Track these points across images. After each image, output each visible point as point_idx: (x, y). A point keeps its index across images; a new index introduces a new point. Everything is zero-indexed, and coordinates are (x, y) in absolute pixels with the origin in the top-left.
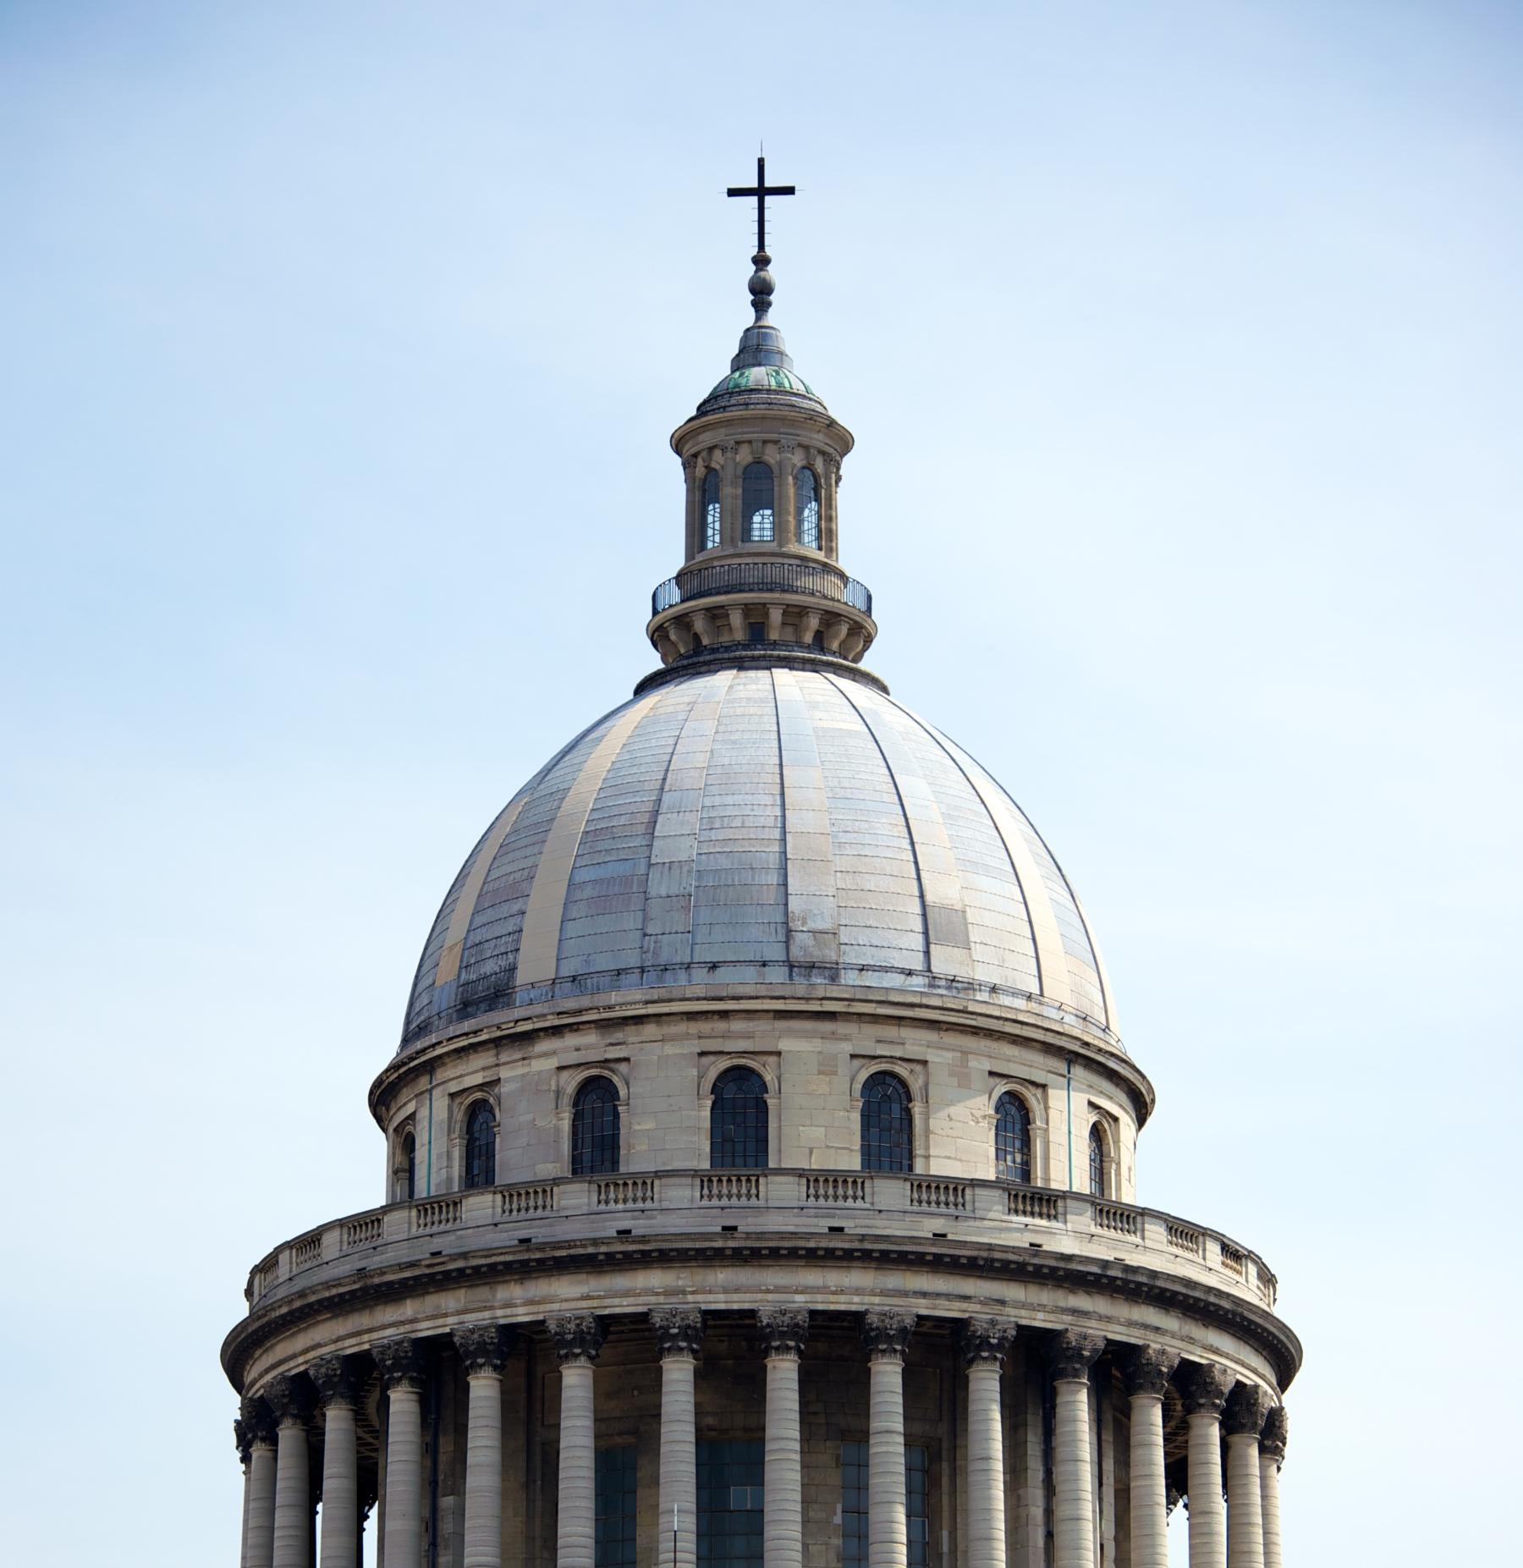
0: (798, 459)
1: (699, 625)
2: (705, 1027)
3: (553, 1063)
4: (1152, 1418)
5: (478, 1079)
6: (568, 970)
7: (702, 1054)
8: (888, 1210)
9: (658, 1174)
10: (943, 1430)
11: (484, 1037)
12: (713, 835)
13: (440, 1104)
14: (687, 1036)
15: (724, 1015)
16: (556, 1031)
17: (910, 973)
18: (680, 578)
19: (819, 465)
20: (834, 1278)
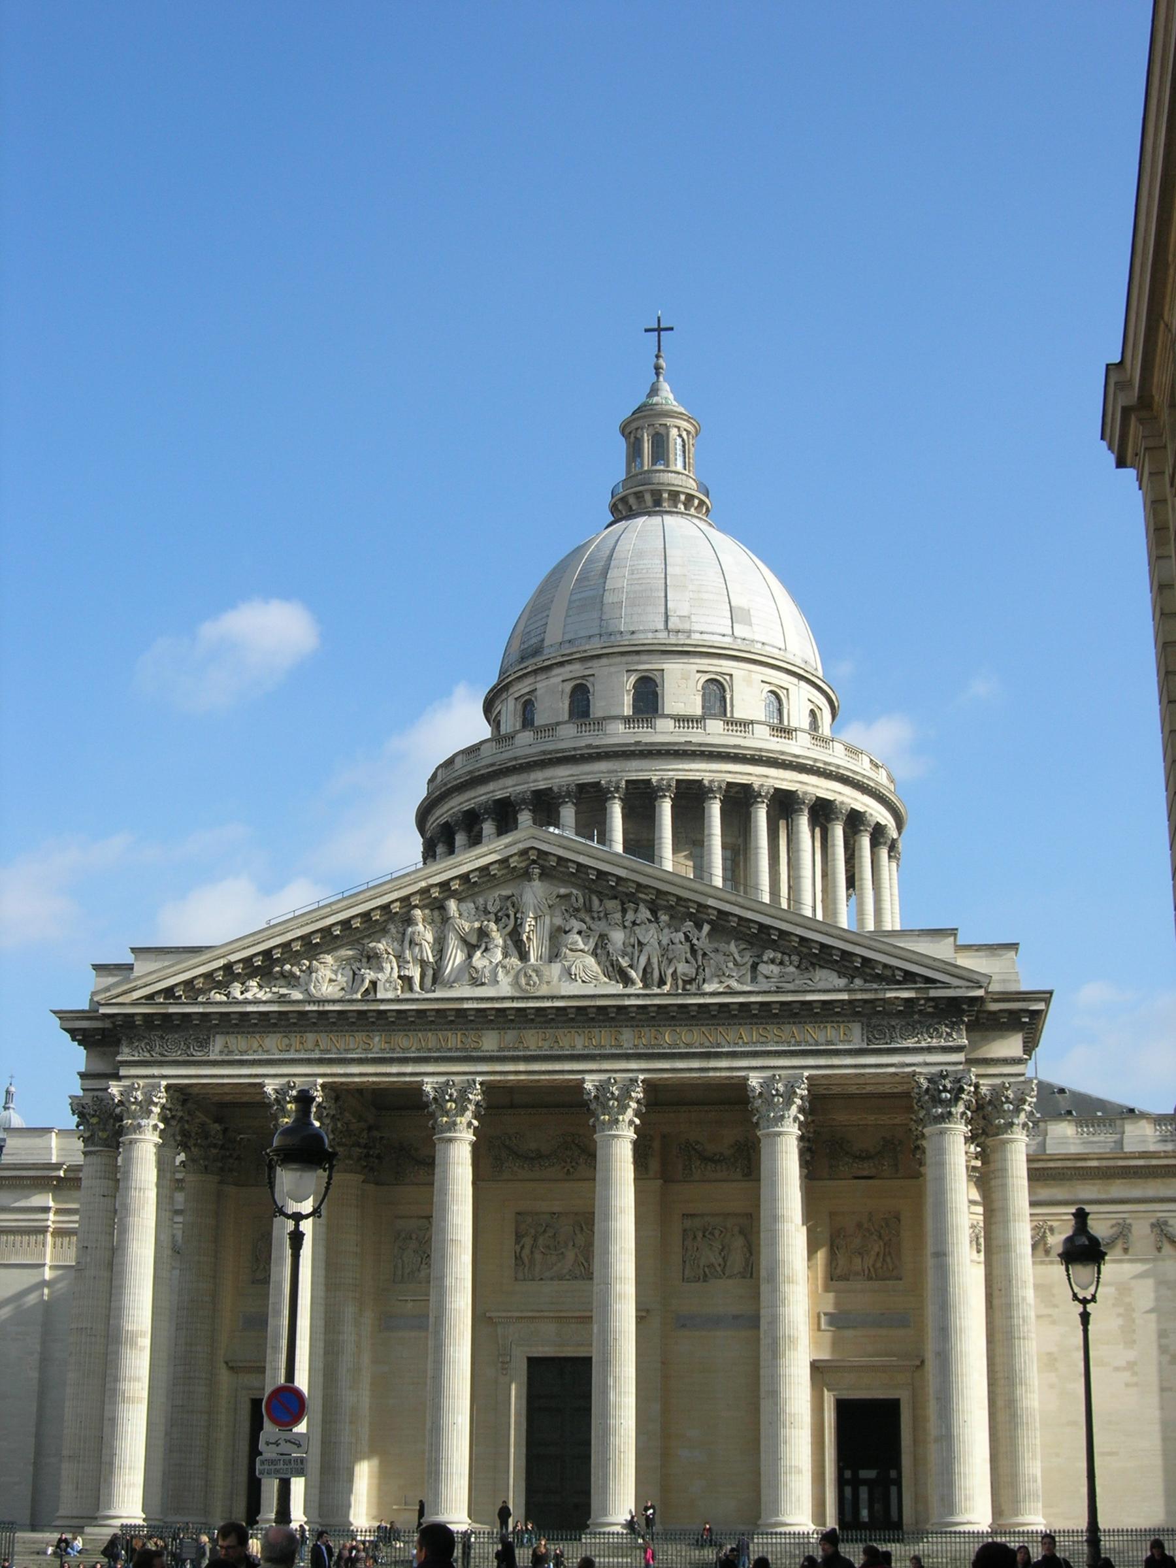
3: (561, 678)
5: (527, 690)
6: (567, 638)
8: (715, 733)
9: (604, 718)
10: (740, 841)
12: (634, 576)
13: (511, 702)
14: (621, 663)
15: (638, 653)
16: (561, 664)
19: (684, 434)
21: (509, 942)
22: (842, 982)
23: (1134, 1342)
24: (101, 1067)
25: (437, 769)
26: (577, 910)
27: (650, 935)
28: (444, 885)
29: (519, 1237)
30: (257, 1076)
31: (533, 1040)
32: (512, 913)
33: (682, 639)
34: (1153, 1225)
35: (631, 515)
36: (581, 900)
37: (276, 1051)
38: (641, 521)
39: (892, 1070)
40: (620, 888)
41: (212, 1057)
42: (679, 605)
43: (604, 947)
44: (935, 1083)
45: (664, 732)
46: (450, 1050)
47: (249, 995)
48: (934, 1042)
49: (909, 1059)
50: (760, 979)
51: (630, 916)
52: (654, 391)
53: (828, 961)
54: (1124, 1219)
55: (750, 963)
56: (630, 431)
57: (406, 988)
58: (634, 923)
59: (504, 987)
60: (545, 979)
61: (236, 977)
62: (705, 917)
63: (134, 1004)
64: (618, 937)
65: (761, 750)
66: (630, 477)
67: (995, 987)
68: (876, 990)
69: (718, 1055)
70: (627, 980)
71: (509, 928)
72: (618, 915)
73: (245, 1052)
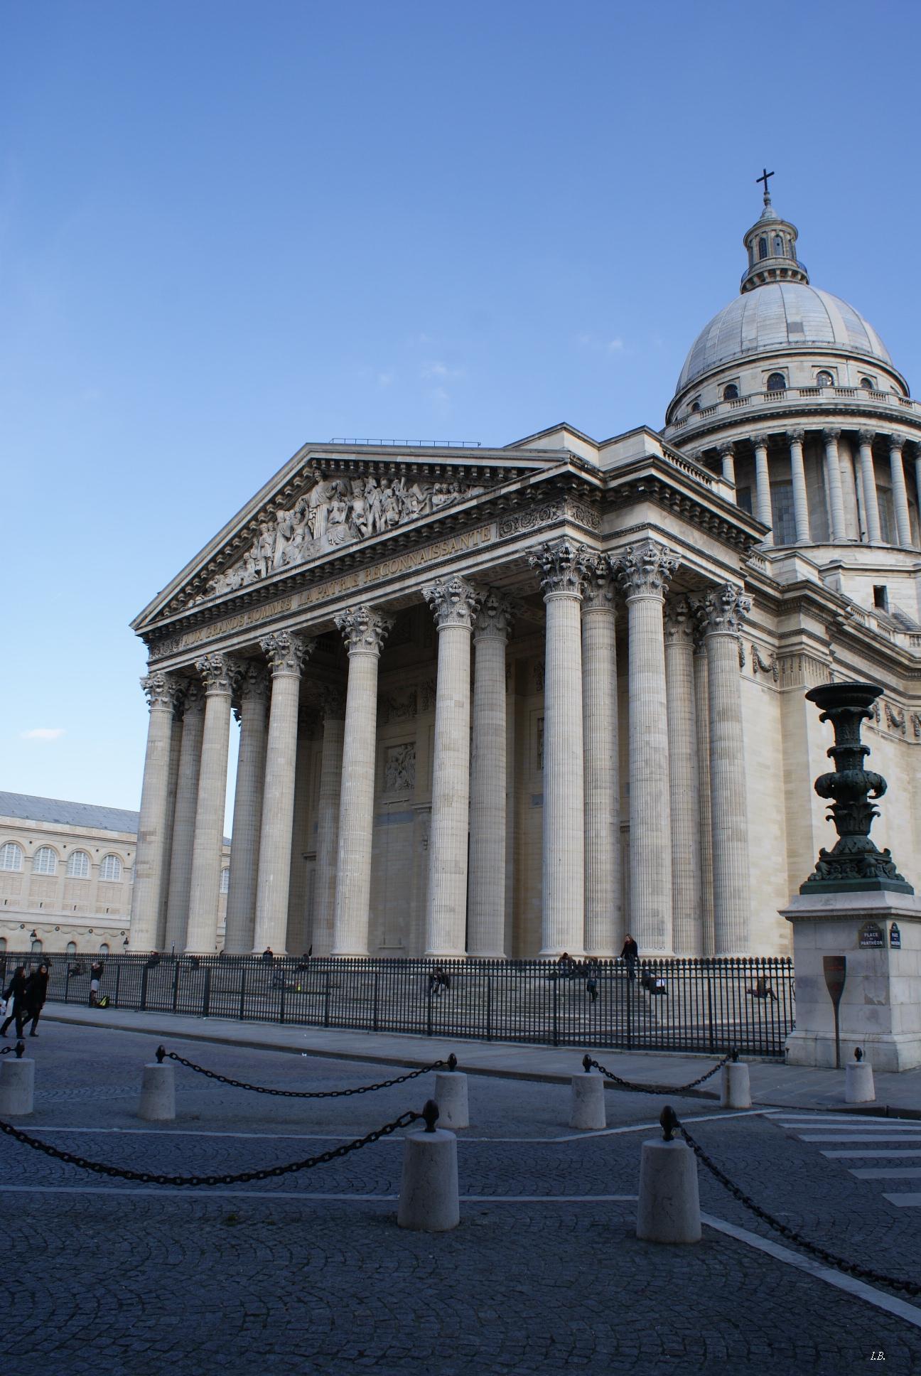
0: (773, 234)
15: (722, 371)
19: (781, 234)
27: (374, 498)
42: (749, 333)
48: (544, 524)
59: (299, 562)
61: (190, 596)
64: (358, 505)
70: (363, 535)
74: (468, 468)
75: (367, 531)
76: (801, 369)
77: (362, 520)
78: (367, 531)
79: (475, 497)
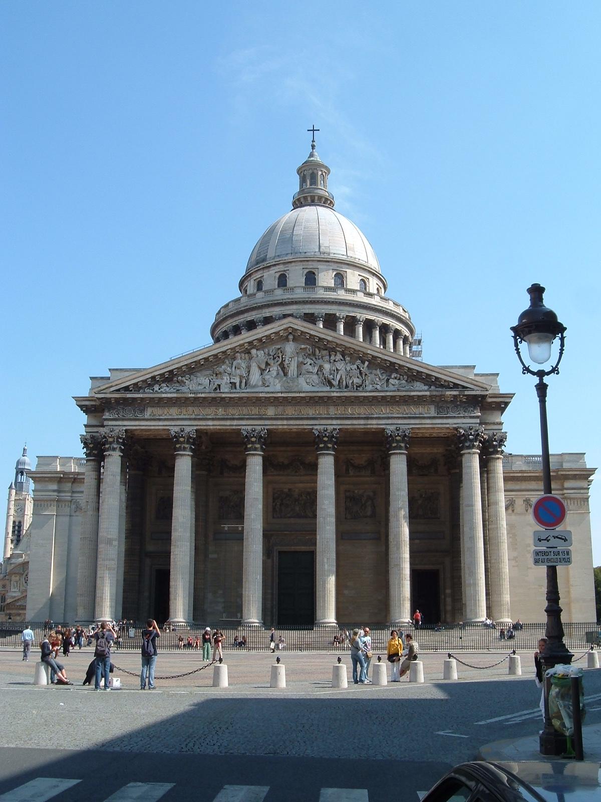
0: (320, 173)
1: (302, 200)
2: (304, 263)
4: (391, 338)
5: (260, 276)
6: (277, 255)
7: (303, 268)
8: (341, 295)
11: (261, 267)
13: (252, 281)
15: (308, 261)
17: (343, 255)
18: (299, 193)
19: (324, 174)
20: (329, 307)
21: (279, 368)
22: (426, 388)
23: (516, 549)
24: (94, 422)
25: (221, 309)
26: (309, 355)
28: (250, 343)
29: (274, 499)
30: (166, 425)
31: (290, 411)
32: (280, 355)
33: (326, 256)
34: (524, 501)
35: (302, 206)
36: (311, 350)
37: (175, 415)
38: (307, 208)
39: (448, 426)
40: (328, 345)
41: (146, 417)
42: (325, 242)
43: (321, 371)
44: (467, 432)
45: (321, 294)
46: (253, 415)
47: (161, 390)
49: (455, 421)
50: (390, 385)
51: (333, 358)
52: (311, 155)
53: (420, 379)
54: (512, 498)
55: (386, 379)
56: (300, 171)
57: (233, 387)
58: (335, 361)
59: (278, 387)
60: (296, 384)
62: (366, 359)
63: (111, 393)
64: (327, 366)
65: (360, 302)
66: (302, 191)
67: (490, 392)
68: (442, 391)
69: (372, 418)
70: (331, 385)
71: (279, 362)
72: (328, 357)
73: (161, 415)
74: (418, 372)
75: (335, 383)
76: (354, 275)
77: (332, 376)
78: (335, 383)
79: (420, 389)
